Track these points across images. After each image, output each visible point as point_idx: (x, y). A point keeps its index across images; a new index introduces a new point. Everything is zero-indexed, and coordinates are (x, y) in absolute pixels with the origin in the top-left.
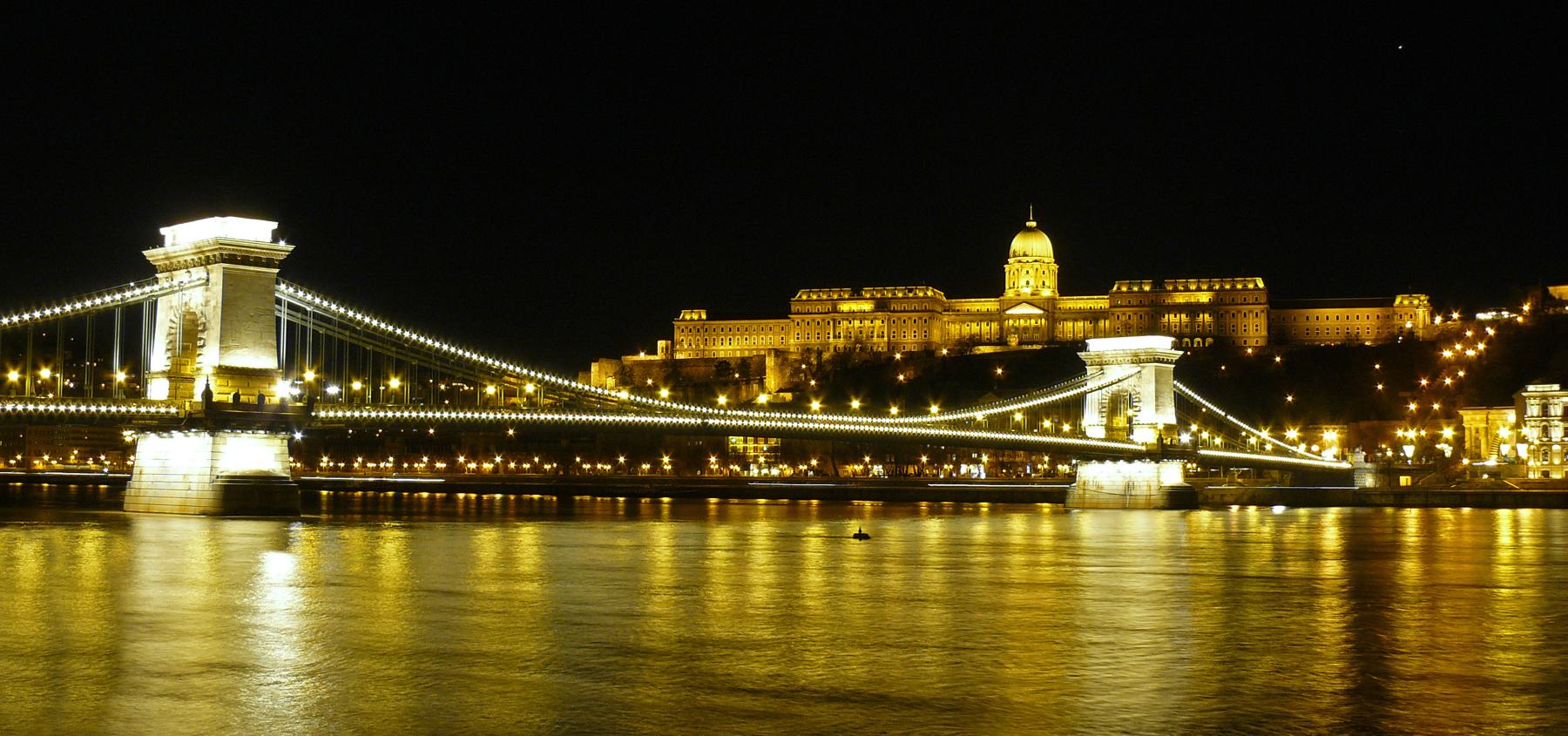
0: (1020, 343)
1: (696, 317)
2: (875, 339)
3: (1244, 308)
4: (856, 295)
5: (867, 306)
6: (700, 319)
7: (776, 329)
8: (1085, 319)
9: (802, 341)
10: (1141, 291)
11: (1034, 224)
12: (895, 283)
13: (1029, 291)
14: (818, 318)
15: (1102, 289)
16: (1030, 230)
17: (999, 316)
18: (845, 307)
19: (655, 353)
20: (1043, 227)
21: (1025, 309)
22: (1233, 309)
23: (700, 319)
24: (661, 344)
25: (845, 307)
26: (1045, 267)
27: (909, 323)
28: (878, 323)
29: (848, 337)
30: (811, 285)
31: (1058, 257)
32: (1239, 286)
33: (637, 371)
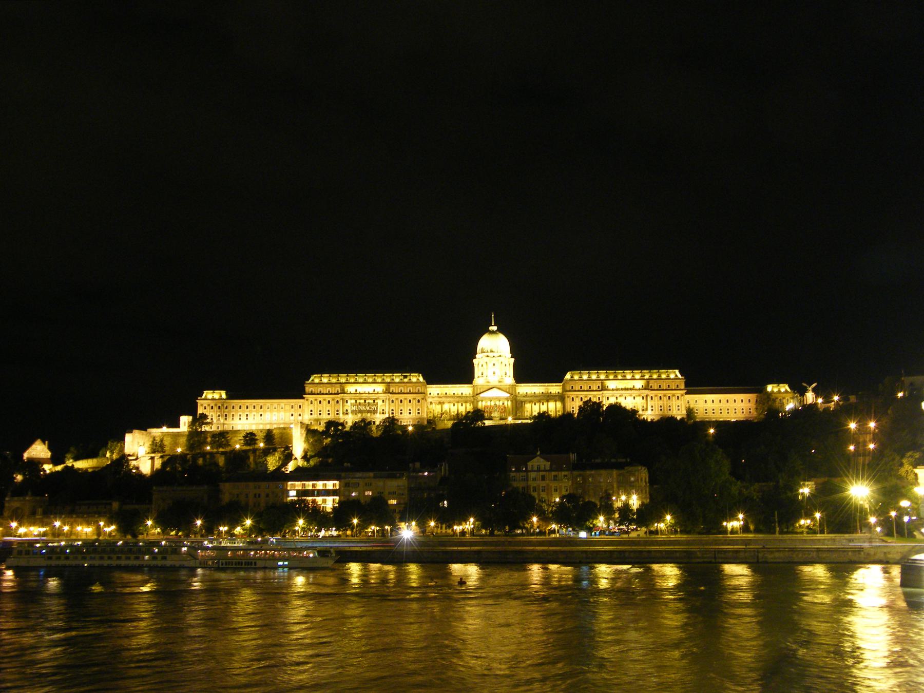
1: (216, 396)
6: (221, 399)
7: (288, 407)
9: (315, 416)
10: (589, 380)
11: (495, 328)
12: (393, 370)
15: (558, 379)
16: (493, 332)
19: (179, 427)
20: (501, 330)
21: (495, 393)
23: (221, 399)
24: (185, 420)
25: (350, 388)
30: (321, 371)
31: (514, 353)
33: (167, 442)
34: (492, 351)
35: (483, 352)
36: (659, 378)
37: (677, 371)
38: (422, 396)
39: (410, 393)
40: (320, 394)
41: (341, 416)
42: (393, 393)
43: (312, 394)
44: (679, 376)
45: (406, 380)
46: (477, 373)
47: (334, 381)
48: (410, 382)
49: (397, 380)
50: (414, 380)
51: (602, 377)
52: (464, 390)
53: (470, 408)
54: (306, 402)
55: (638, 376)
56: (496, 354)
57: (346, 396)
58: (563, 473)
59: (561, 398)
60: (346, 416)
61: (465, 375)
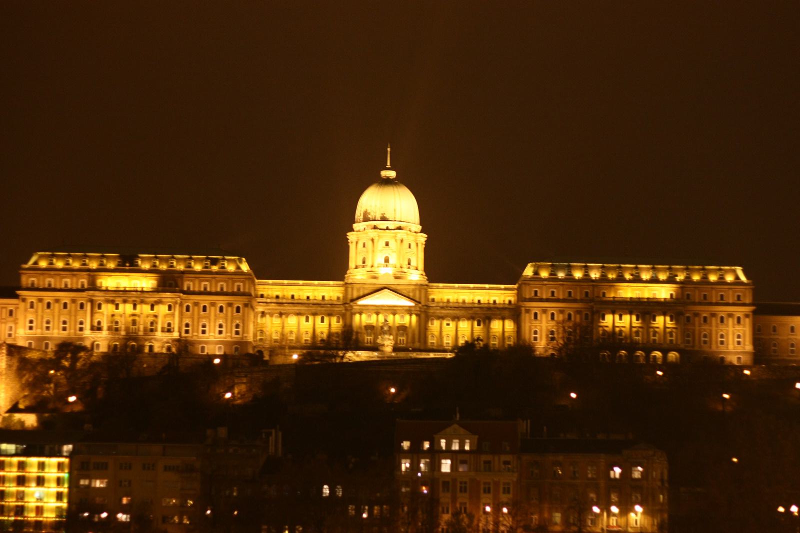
0: (396, 349)
2: (159, 334)
3: (722, 310)
4: (128, 264)
5: (147, 282)
8: (471, 318)
9: (37, 332)
10: (570, 278)
11: (392, 174)
12: (190, 249)
13: (390, 271)
14: (65, 297)
16: (388, 182)
17: (345, 307)
18: (109, 282)
21: (386, 299)
22: (705, 311)
25: (109, 282)
26: (409, 238)
27: (212, 311)
28: (162, 309)
29: (114, 329)
32: (713, 278)
34: (384, 219)
35: (366, 219)
36: (705, 280)
37: (739, 271)
38: (244, 299)
39: (221, 293)
40: (49, 289)
41: (87, 332)
42: (189, 292)
43: (33, 288)
44: (743, 278)
45: (215, 268)
46: (354, 258)
47: (76, 265)
48: (223, 272)
49: (198, 267)
50: (231, 268)
51: (595, 275)
52: (327, 291)
53: (336, 324)
54: (22, 305)
55: (662, 276)
56: (391, 225)
57: (99, 297)
58: (504, 458)
59: (513, 312)
60: (97, 334)
61: (331, 262)
